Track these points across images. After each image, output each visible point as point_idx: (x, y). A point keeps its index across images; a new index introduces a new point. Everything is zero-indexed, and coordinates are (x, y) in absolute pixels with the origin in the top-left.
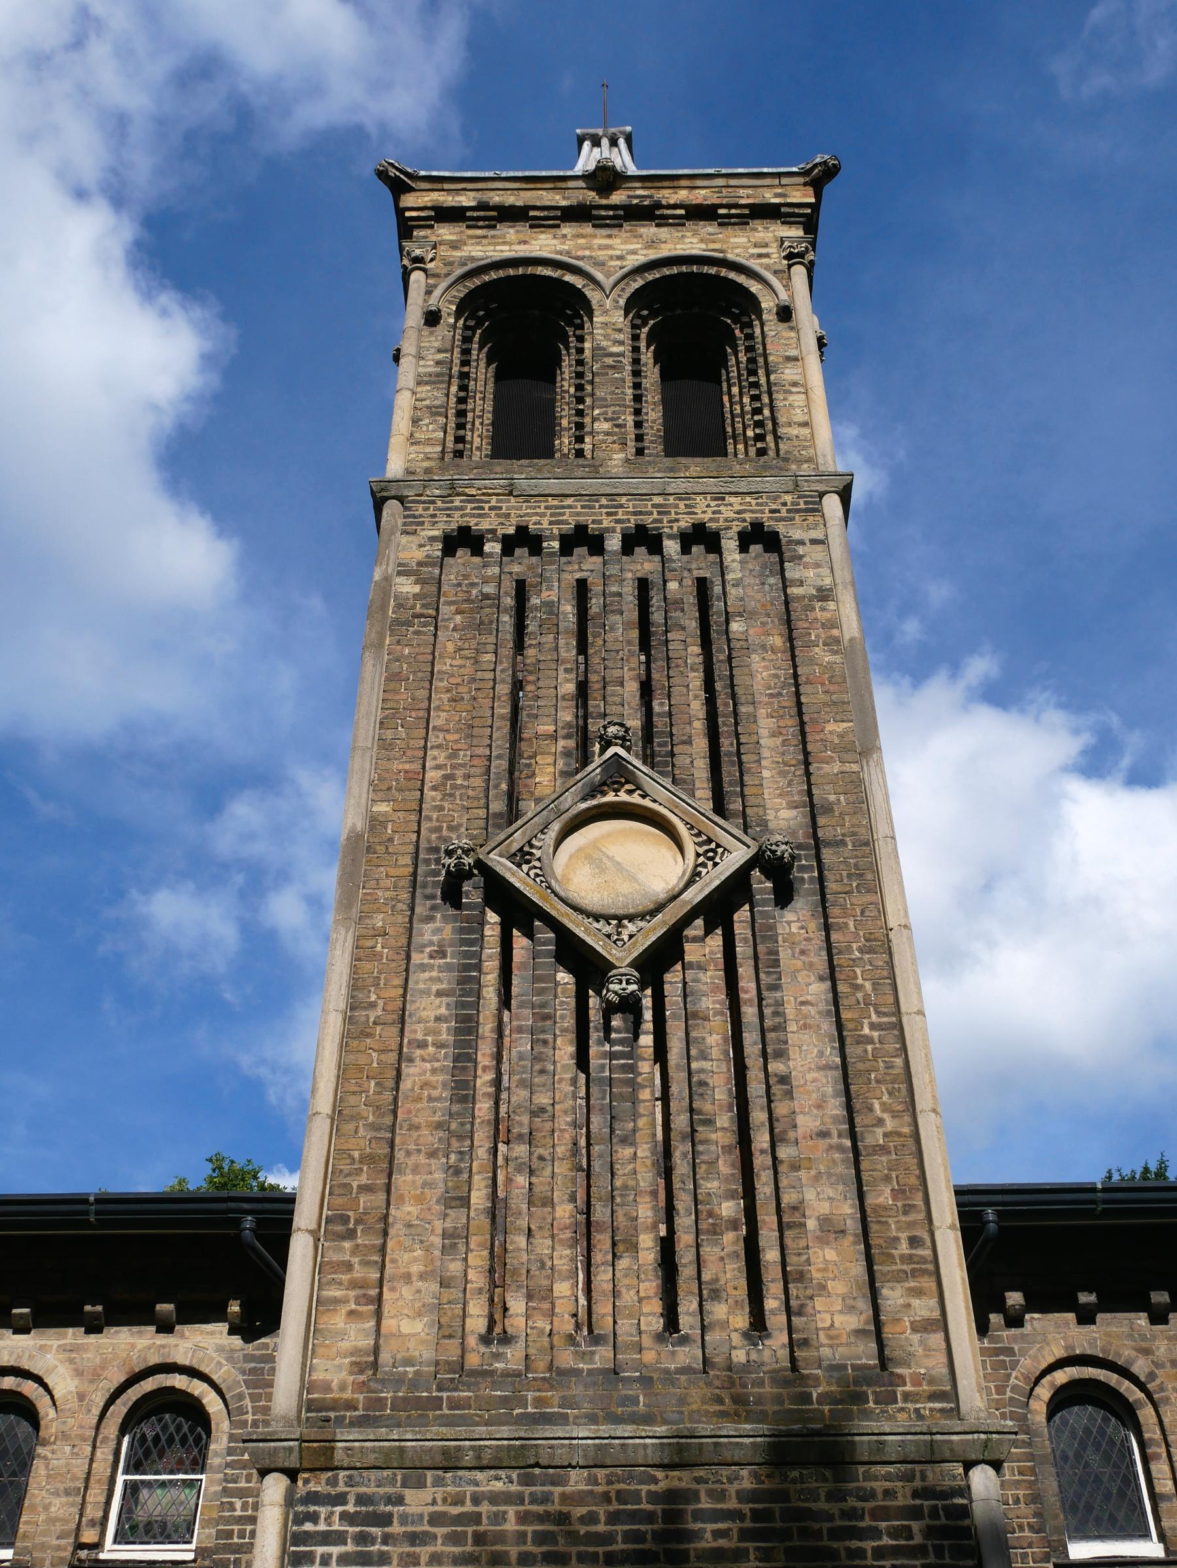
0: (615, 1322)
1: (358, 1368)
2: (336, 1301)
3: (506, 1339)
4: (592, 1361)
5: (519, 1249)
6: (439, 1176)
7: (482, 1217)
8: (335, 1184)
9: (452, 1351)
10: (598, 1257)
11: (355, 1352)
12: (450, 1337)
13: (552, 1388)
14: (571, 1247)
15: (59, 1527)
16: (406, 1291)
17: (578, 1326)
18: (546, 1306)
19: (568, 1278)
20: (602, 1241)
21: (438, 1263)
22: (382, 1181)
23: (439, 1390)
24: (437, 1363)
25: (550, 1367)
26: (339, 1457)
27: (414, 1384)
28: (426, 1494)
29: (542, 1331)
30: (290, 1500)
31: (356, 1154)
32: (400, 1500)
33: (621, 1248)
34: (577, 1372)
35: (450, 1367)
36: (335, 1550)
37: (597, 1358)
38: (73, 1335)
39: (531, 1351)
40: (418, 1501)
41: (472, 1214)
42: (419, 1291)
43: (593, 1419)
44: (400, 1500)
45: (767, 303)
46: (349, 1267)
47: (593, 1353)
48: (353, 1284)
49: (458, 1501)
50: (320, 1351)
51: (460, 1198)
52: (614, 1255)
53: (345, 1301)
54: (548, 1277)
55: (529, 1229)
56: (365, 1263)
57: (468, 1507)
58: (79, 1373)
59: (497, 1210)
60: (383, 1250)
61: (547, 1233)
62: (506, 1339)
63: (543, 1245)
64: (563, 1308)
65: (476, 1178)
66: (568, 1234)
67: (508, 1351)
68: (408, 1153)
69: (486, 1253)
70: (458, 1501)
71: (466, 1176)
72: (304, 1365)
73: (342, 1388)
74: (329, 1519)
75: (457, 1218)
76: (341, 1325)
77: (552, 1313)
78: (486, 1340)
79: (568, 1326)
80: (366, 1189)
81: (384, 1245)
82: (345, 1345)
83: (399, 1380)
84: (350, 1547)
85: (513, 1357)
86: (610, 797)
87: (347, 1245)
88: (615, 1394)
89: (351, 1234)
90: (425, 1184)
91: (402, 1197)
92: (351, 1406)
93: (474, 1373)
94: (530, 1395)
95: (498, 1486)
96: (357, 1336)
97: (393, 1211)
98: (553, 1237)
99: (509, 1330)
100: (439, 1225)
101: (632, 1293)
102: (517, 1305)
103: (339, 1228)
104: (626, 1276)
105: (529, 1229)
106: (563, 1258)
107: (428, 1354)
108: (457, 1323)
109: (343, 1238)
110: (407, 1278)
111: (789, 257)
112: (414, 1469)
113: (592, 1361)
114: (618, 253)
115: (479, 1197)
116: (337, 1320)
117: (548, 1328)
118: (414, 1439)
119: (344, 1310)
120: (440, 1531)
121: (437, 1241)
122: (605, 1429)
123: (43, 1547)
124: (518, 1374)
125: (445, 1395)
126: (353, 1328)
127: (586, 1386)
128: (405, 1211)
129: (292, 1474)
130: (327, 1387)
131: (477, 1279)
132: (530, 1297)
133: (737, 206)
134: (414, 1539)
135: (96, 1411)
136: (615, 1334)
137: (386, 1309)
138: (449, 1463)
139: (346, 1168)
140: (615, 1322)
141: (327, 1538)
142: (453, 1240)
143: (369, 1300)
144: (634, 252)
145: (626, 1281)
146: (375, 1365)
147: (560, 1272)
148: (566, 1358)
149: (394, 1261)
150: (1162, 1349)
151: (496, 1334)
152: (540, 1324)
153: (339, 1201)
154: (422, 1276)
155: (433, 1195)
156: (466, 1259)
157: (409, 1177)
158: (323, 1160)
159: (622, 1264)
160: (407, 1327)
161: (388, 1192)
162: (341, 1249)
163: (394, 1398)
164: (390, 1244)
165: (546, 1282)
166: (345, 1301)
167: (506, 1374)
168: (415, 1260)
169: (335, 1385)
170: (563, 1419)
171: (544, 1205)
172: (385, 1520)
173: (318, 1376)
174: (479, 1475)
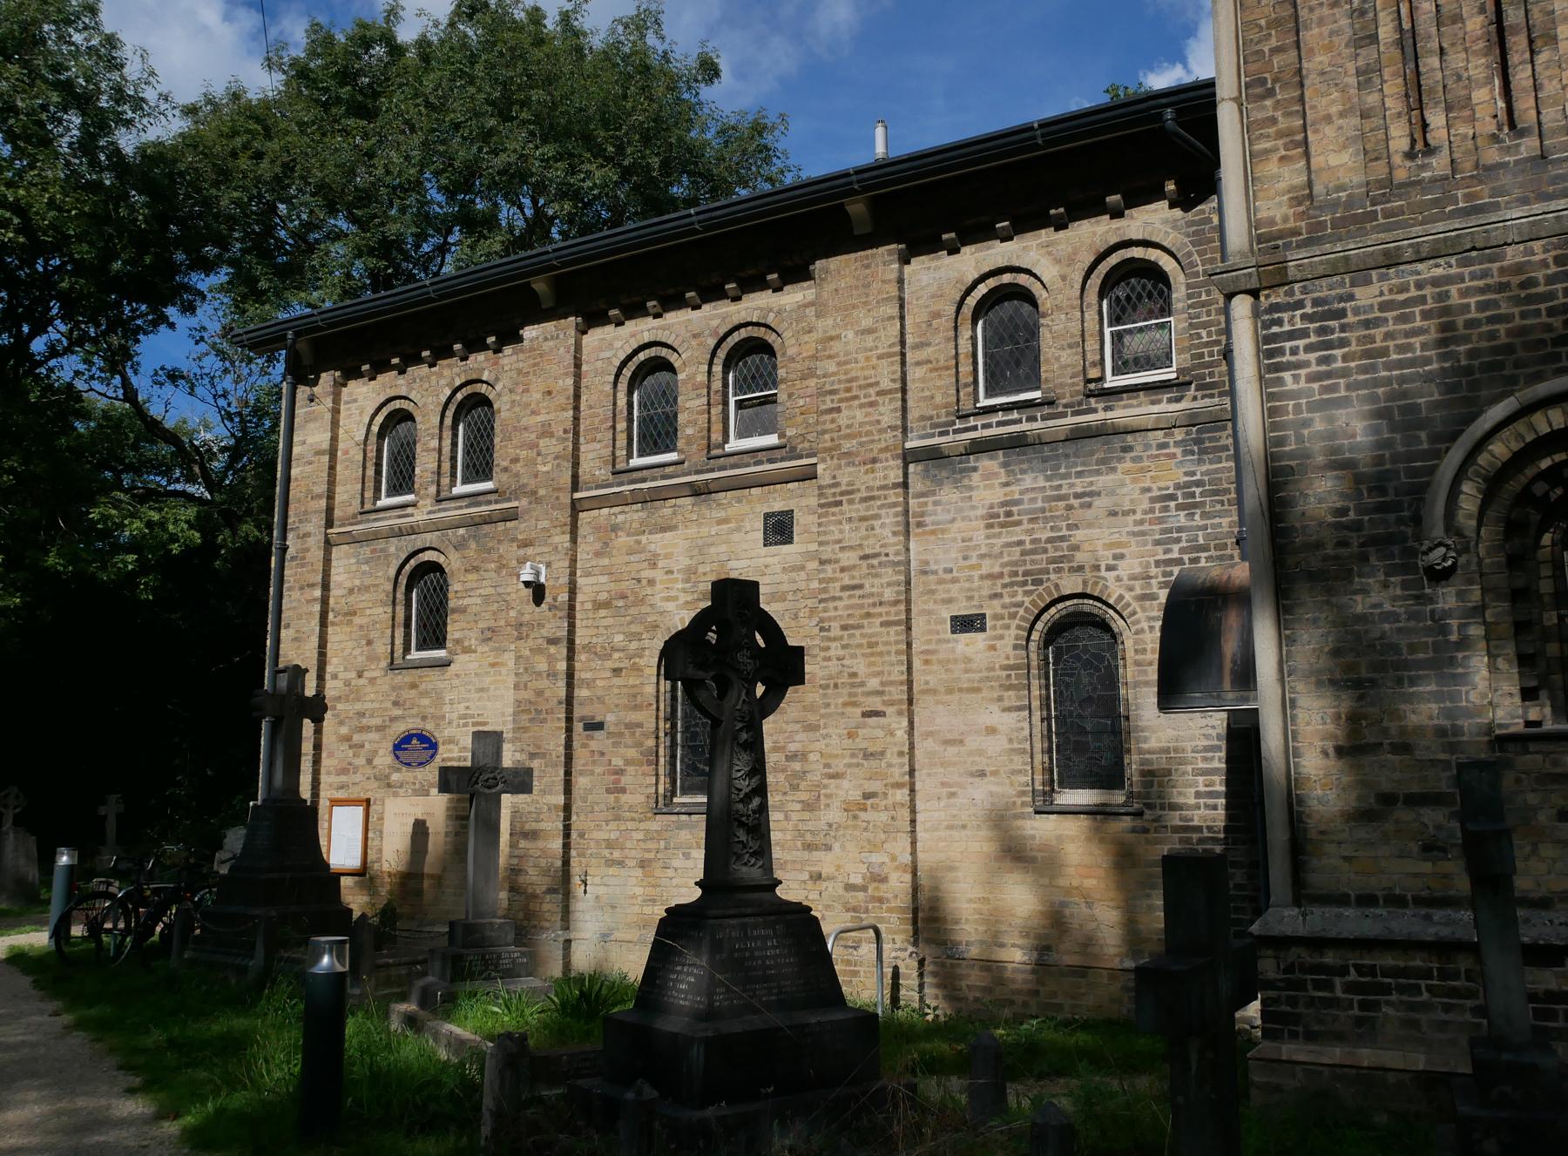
0: (1539, 113)
1: (1297, 201)
2: (1267, 151)
3: (1429, 150)
4: (1518, 153)
5: (1433, 70)
6: (1344, 22)
7: (1392, 49)
8: (1248, 53)
9: (1380, 170)
10: (1514, 58)
11: (1292, 189)
12: (1377, 159)
13: (1481, 182)
14: (1486, 55)
15: (1070, 371)
16: (1329, 131)
17: (1500, 129)
18: (1466, 113)
19: (1485, 85)
20: (1517, 43)
21: (1356, 100)
22: (1291, 40)
23: (1373, 204)
24: (1368, 183)
25: (1477, 167)
26: (1292, 272)
27: (1350, 203)
28: (1374, 289)
29: (1465, 136)
30: (1256, 313)
31: (1263, 22)
32: (1351, 297)
33: (1538, 43)
34: (1504, 165)
35: (1380, 184)
36: (1301, 343)
37: (1523, 149)
38: (1046, 235)
39: (1455, 156)
40: (1367, 296)
41: (1382, 49)
42: (1341, 128)
43: (1524, 201)
44: (1351, 297)
46: (1274, 121)
47: (1518, 145)
48: (1280, 135)
49: (1403, 289)
50: (1260, 194)
51: (1369, 37)
52: (1532, 52)
53: (1275, 150)
54: (1466, 87)
55: (1442, 49)
56: (1288, 114)
57: (1413, 293)
58: (1058, 261)
59: (1409, 43)
60: (1302, 99)
61: (1460, 48)
62: (1429, 150)
63: (1456, 60)
64: (1483, 113)
65: (1381, 15)
66: (1481, 44)
67: (1434, 161)
68: (1311, 9)
69: (1400, 80)
70: (1403, 289)
71: (1371, 15)
72: (1248, 209)
73: (1285, 219)
74: (1292, 321)
75: (1368, 55)
76: (1275, 170)
77: (1473, 119)
78: (1410, 155)
79: (1491, 127)
80: (1276, 51)
81: (1302, 96)
82: (1282, 185)
83: (1335, 204)
84: (1313, 339)
85: (1439, 164)
87: (1268, 103)
88: (1545, 176)
89: (1270, 93)
90: (1331, 34)
91: (1312, 50)
92: (1295, 232)
93: (1402, 185)
94: (1460, 194)
95: (1439, 272)
96: (1292, 176)
97: (1305, 65)
98: (1466, 50)
99: (1432, 142)
100: (1351, 67)
101: (1555, 82)
102: (1436, 119)
103: (1259, 90)
104: (1547, 68)
105: (1442, 49)
106: (1479, 66)
107: (1358, 178)
108: (1382, 145)
109: (1263, 97)
110: (1328, 119)
112: (1360, 272)
113: (1518, 153)
115: (1386, 32)
116: (1272, 167)
117: (1471, 132)
118: (1354, 248)
119: (1275, 157)
120: (1390, 315)
121: (1353, 81)
122: (1537, 207)
123: (1062, 385)
124: (1445, 178)
125: (1379, 208)
126: (1286, 171)
127: (1515, 175)
128: (1316, 62)
129: (1254, 293)
130: (1272, 222)
131: (1394, 105)
132: (1449, 108)
134: (1367, 324)
135: (1078, 286)
136: (1540, 124)
137: (1312, 149)
138: (1391, 261)
139: (1255, 37)
140: (1539, 113)
141: (1292, 335)
142: (1367, 76)
143: (1297, 145)
145: (1548, 73)
146: (1311, 196)
147: (1477, 81)
148: (1492, 155)
149: (1313, 107)
151: (1421, 147)
152: (1462, 130)
153: (1253, 67)
154: (1342, 115)
155: (1340, 41)
156: (1381, 90)
157: (1316, 31)
158: (1233, 35)
159: (1541, 58)
160: (1334, 160)
161: (1298, 48)
162: (1264, 108)
163: (1332, 220)
164: (1307, 94)
165: (1463, 93)
166: (1275, 150)
167: (1434, 180)
168: (1333, 101)
169: (1278, 219)
170: (1495, 207)
171: (1454, 22)
172: (1341, 314)
173: (1262, 215)
174: (1420, 266)
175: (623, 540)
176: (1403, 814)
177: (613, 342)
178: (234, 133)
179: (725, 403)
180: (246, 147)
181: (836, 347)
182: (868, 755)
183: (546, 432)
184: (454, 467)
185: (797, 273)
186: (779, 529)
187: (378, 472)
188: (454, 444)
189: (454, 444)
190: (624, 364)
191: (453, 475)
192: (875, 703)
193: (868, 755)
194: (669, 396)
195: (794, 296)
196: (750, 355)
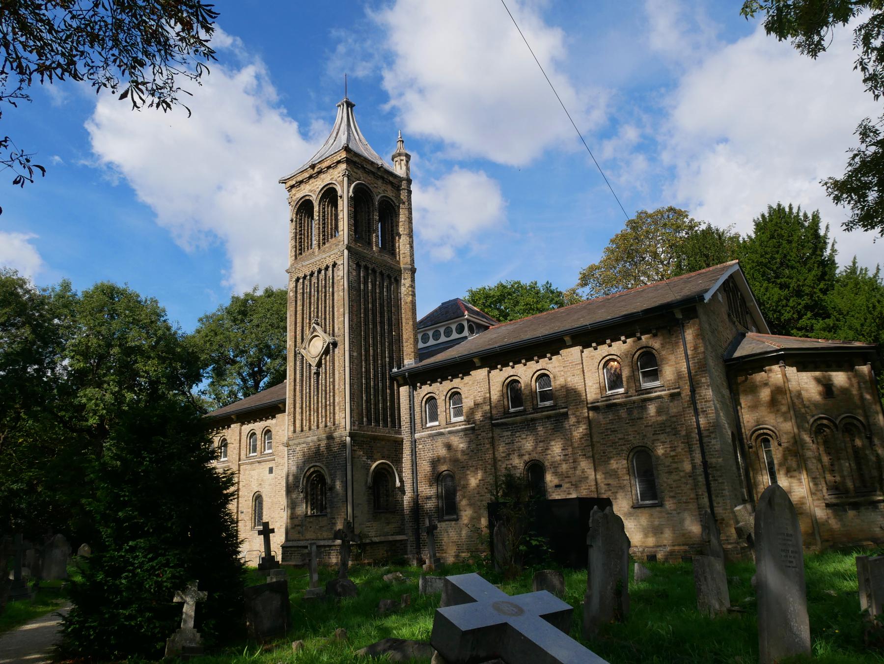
40: (298, 449)
118: (296, 442)
150: (441, 389)
175: (247, 472)
177: (247, 428)
178: (207, 336)
180: (209, 340)
185: (274, 417)
186: (271, 470)
194: (256, 440)
195: (274, 421)
196: (267, 432)
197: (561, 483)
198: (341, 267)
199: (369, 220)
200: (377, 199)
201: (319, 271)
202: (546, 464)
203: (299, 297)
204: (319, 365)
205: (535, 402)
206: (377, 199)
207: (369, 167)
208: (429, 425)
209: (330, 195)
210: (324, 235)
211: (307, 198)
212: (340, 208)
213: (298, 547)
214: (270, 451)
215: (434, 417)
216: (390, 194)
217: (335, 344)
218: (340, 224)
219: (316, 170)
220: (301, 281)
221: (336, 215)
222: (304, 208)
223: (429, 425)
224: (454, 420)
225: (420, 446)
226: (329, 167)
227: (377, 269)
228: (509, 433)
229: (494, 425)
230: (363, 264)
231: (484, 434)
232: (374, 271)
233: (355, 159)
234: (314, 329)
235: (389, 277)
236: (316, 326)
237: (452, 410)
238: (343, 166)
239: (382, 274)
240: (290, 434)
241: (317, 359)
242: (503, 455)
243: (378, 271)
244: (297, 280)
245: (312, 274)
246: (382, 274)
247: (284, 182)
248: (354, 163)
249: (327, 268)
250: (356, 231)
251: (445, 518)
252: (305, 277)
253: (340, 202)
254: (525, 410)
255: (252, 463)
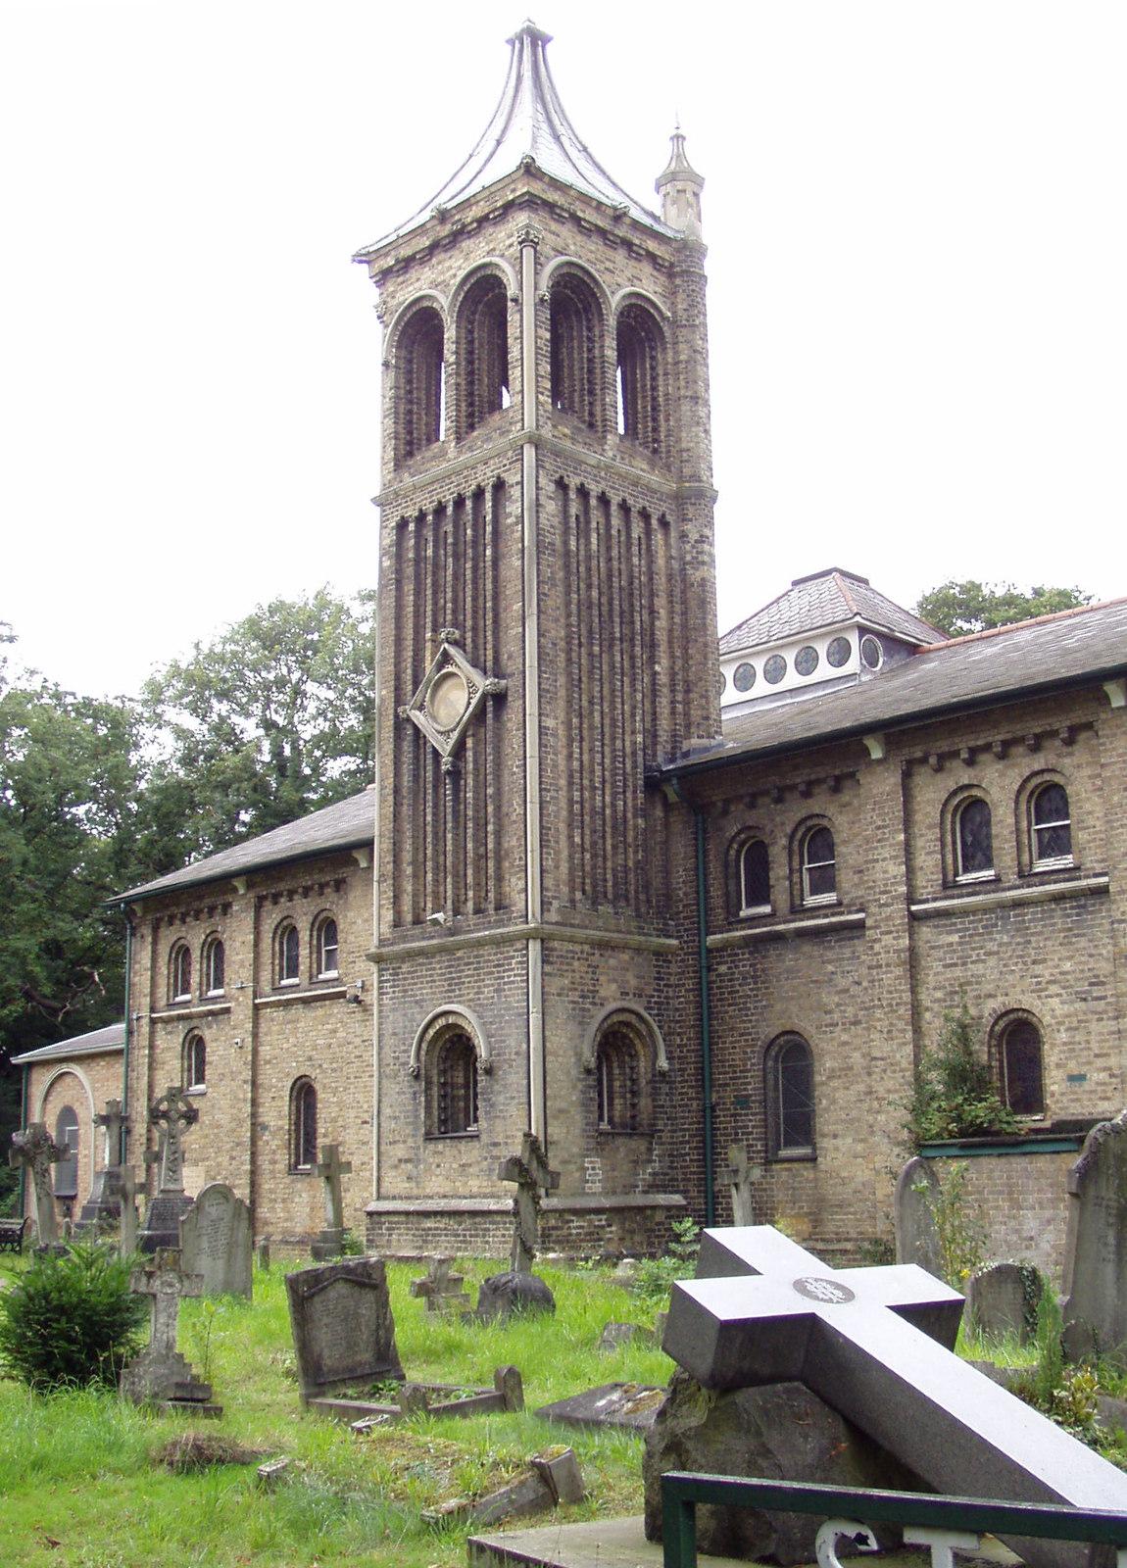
45: (510, 293)
86: (444, 671)
111: (520, 243)
114: (453, 272)
133: (496, 209)
144: (460, 268)
176: (403, 1166)
179: (319, 952)
181: (355, 927)
182: (364, 1143)
183: (242, 966)
184: (208, 980)
187: (176, 980)
188: (209, 967)
189: (209, 967)
190: (277, 927)
191: (208, 985)
192: (366, 1117)
193: (364, 1143)
197: (1084, 1070)
198: (515, 492)
199: (590, 361)
200: (614, 301)
201: (459, 502)
202: (1047, 1020)
203: (410, 571)
204: (459, 751)
205: (1026, 858)
206: (614, 301)
207: (589, 215)
208: (742, 914)
209: (485, 296)
210: (471, 404)
211: (426, 304)
212: (512, 331)
213: (407, 1213)
214: (333, 974)
215: (760, 892)
216: (650, 287)
217: (499, 699)
218: (514, 374)
219: (447, 229)
220: (412, 527)
221: (504, 351)
222: (417, 332)
223: (742, 914)
224: (811, 901)
225: (723, 969)
226: (482, 221)
227: (610, 494)
228: (955, 938)
229: (914, 917)
230: (573, 482)
231: (888, 940)
232: (604, 500)
233: (553, 196)
234: (446, 655)
235: (645, 515)
236: (452, 651)
237: (806, 877)
238: (521, 218)
239: (624, 507)
240: (386, 929)
241: (455, 735)
242: (939, 994)
243: (615, 500)
244: (402, 525)
245: (440, 510)
246: (624, 507)
247: (364, 258)
248: (550, 207)
249: (479, 494)
250: (556, 394)
251: (784, 1153)
252: (421, 518)
253: (512, 318)
254: (997, 880)
255: (287, 1004)
